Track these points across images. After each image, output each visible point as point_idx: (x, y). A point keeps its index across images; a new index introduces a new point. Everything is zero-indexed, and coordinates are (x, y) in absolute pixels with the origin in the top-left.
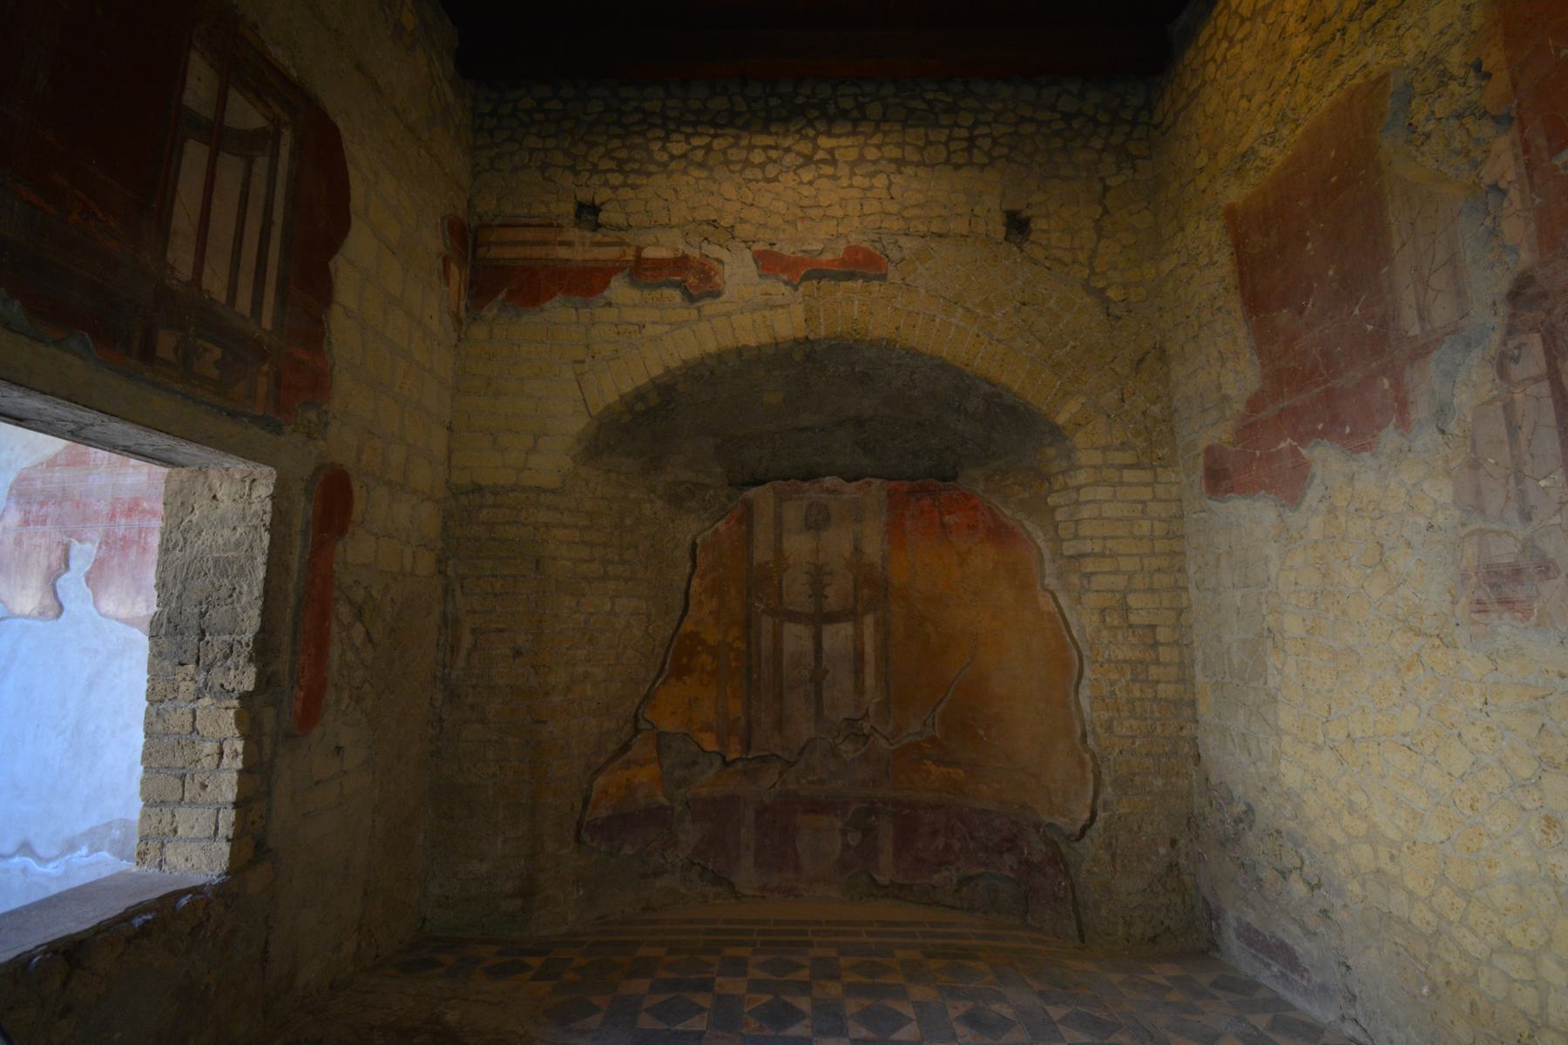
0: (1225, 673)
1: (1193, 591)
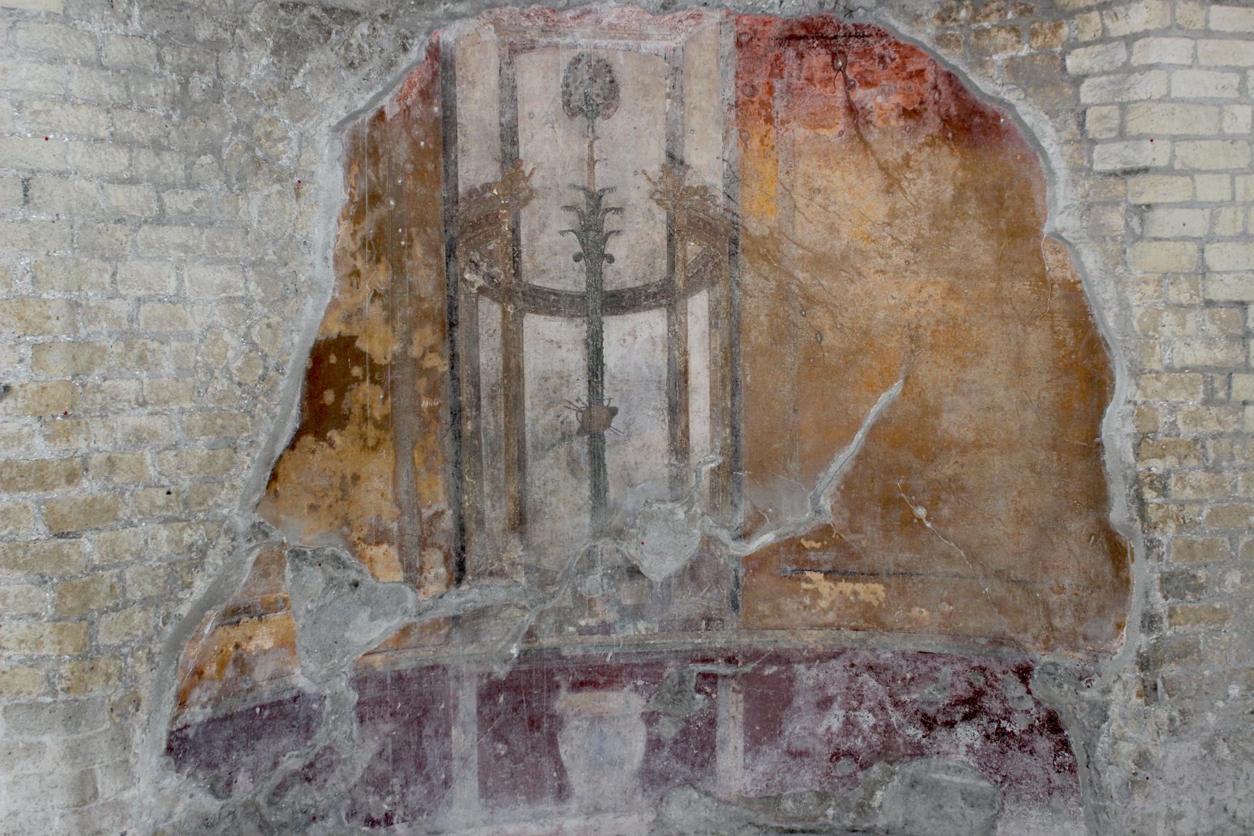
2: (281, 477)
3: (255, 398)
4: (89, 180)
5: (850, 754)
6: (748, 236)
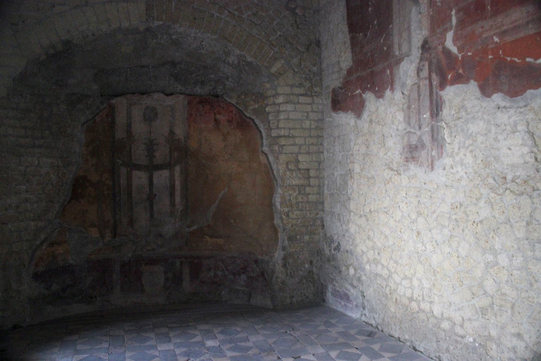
0: (334, 189)
1: (325, 153)
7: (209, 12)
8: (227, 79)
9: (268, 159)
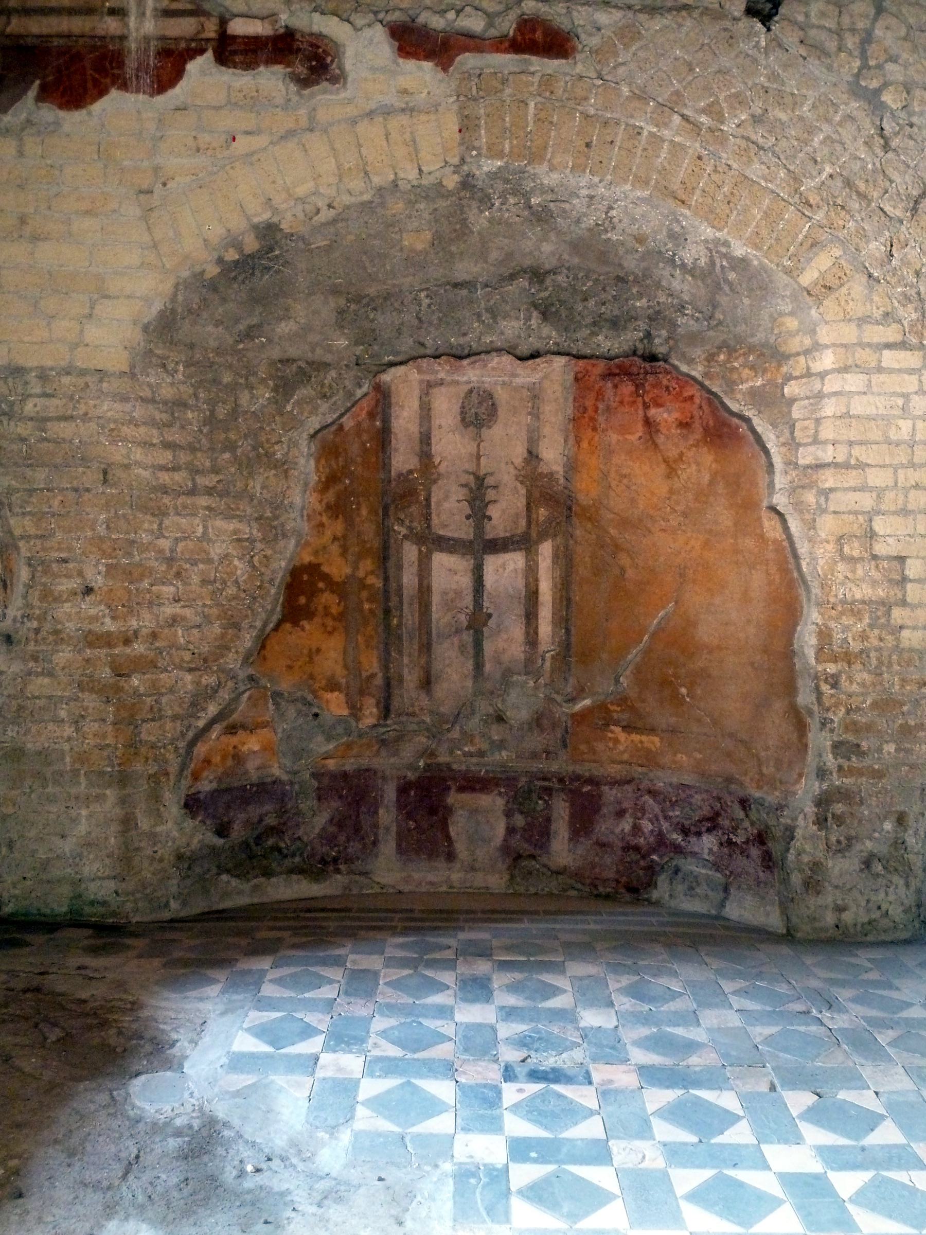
2: (268, 647)
3: (254, 598)
4: (145, 469)
5: (637, 849)
6: (579, 505)
7: (627, 125)
8: (681, 308)
9: (786, 529)
